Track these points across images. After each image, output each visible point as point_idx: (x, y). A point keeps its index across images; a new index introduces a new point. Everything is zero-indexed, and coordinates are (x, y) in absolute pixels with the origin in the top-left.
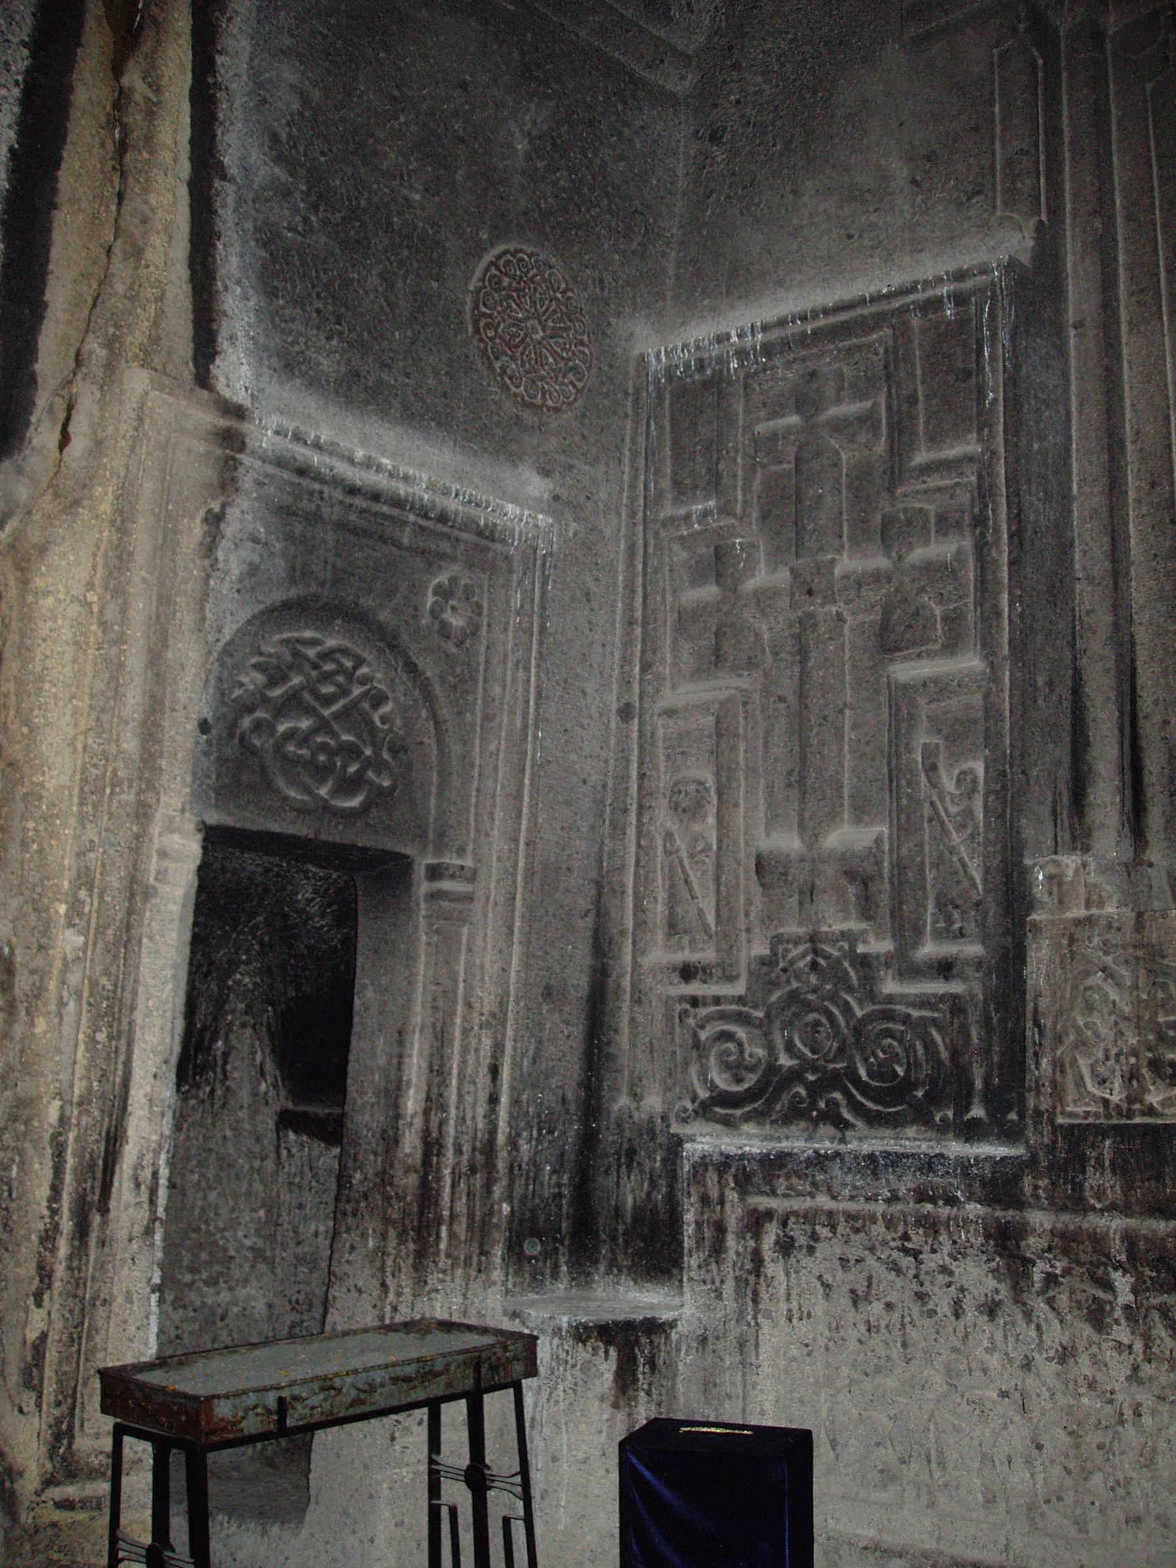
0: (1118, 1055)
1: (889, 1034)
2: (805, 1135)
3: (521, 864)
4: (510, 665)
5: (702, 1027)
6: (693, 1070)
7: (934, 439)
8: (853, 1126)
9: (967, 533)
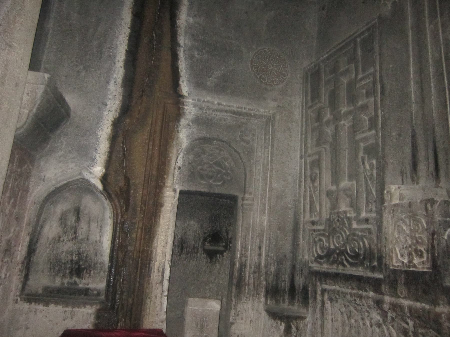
0: (406, 247)
1: (354, 240)
3: (267, 196)
4: (263, 147)
5: (316, 238)
6: (314, 249)
7: (364, 71)
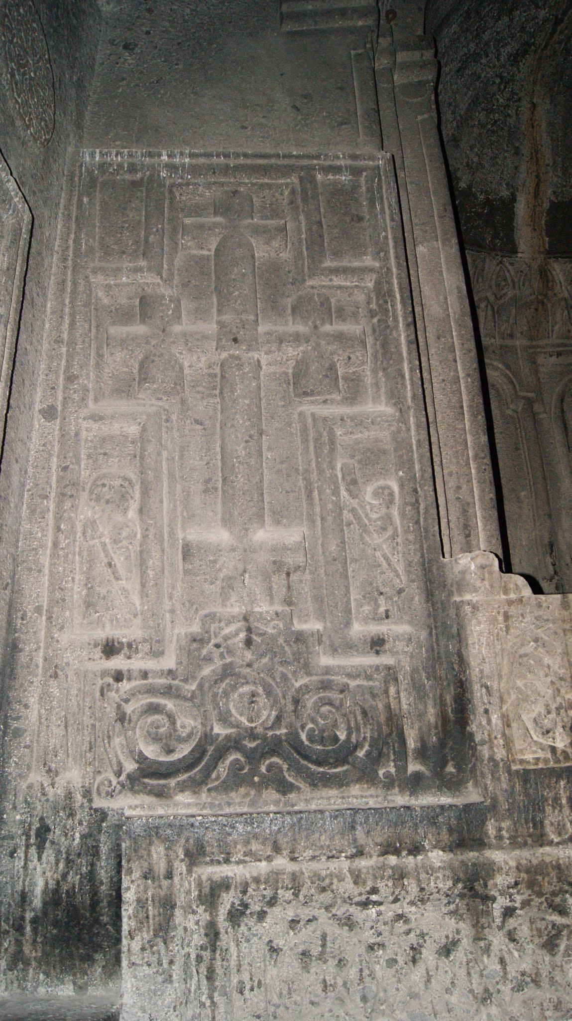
0: (557, 709)
2: (247, 800)
5: (127, 701)
6: (117, 741)
7: (336, 254)
8: (298, 788)
9: (363, 321)
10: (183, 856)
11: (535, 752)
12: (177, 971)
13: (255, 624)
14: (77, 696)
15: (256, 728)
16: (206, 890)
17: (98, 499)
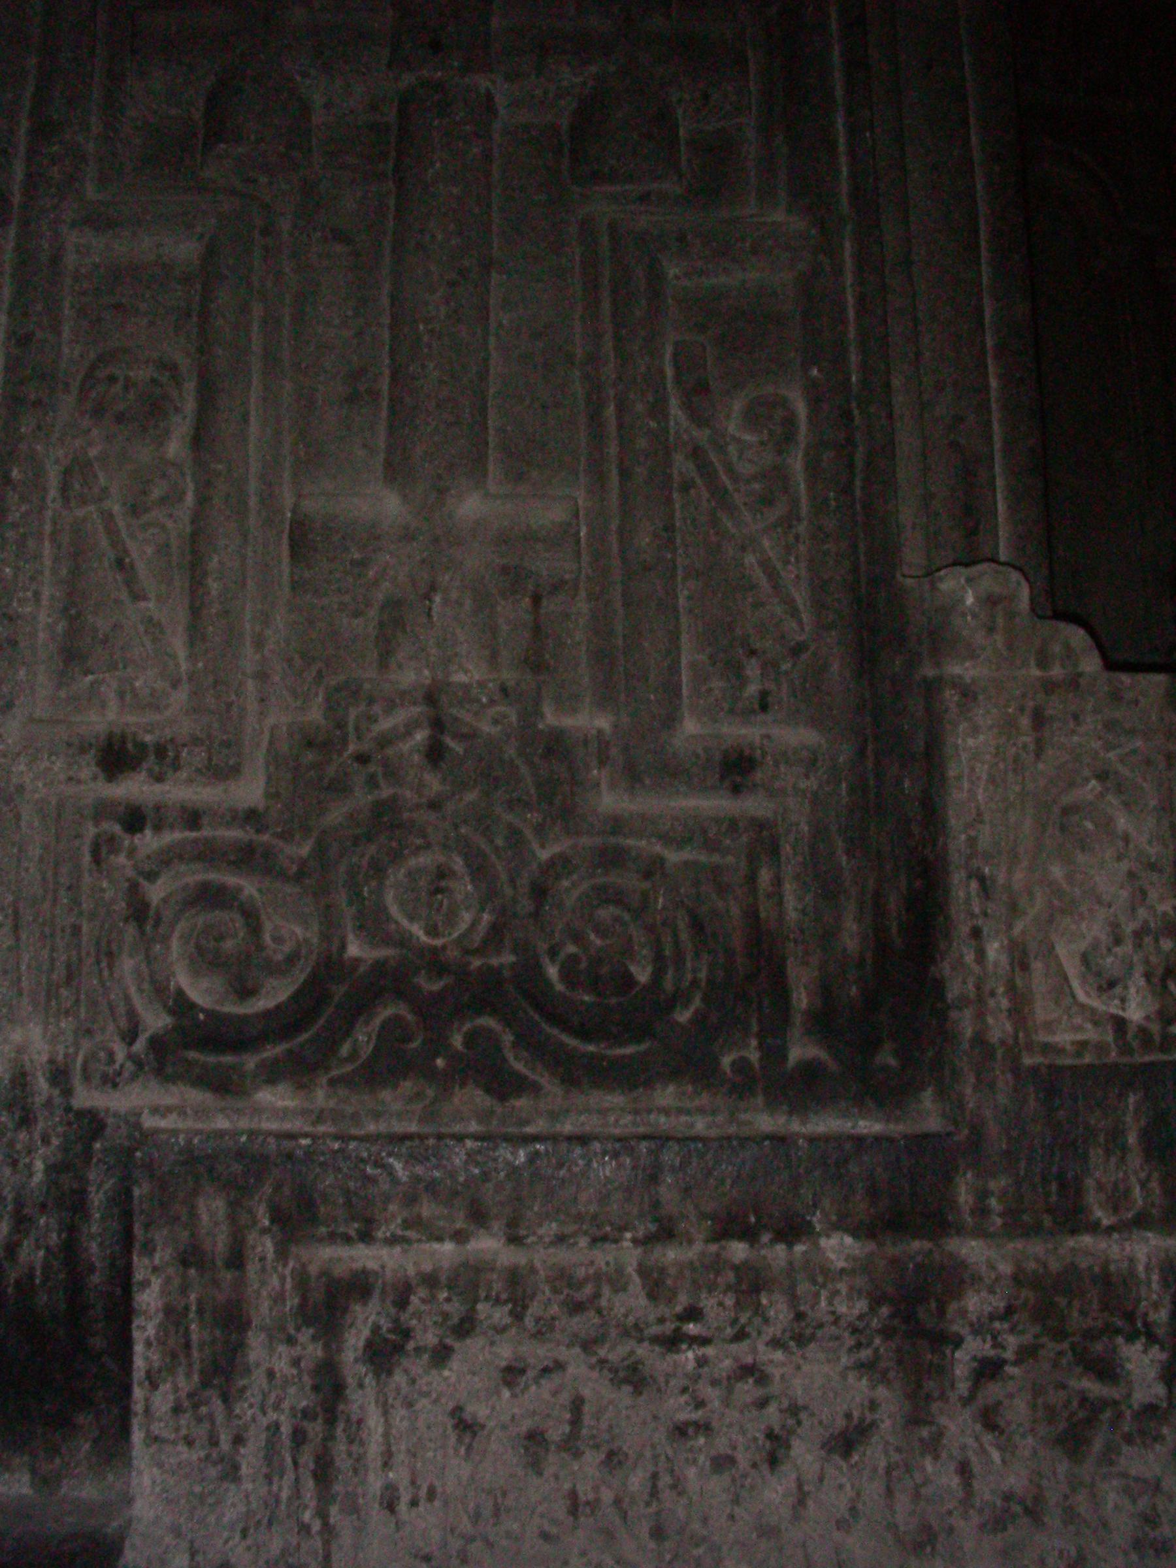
0: (1137, 934)
2: (418, 1106)
5: (151, 876)
6: (127, 965)
10: (267, 1223)
11: (1078, 1029)
12: (250, 1459)
13: (454, 711)
14: (41, 859)
15: (444, 948)
16: (317, 1296)
17: (98, 412)
